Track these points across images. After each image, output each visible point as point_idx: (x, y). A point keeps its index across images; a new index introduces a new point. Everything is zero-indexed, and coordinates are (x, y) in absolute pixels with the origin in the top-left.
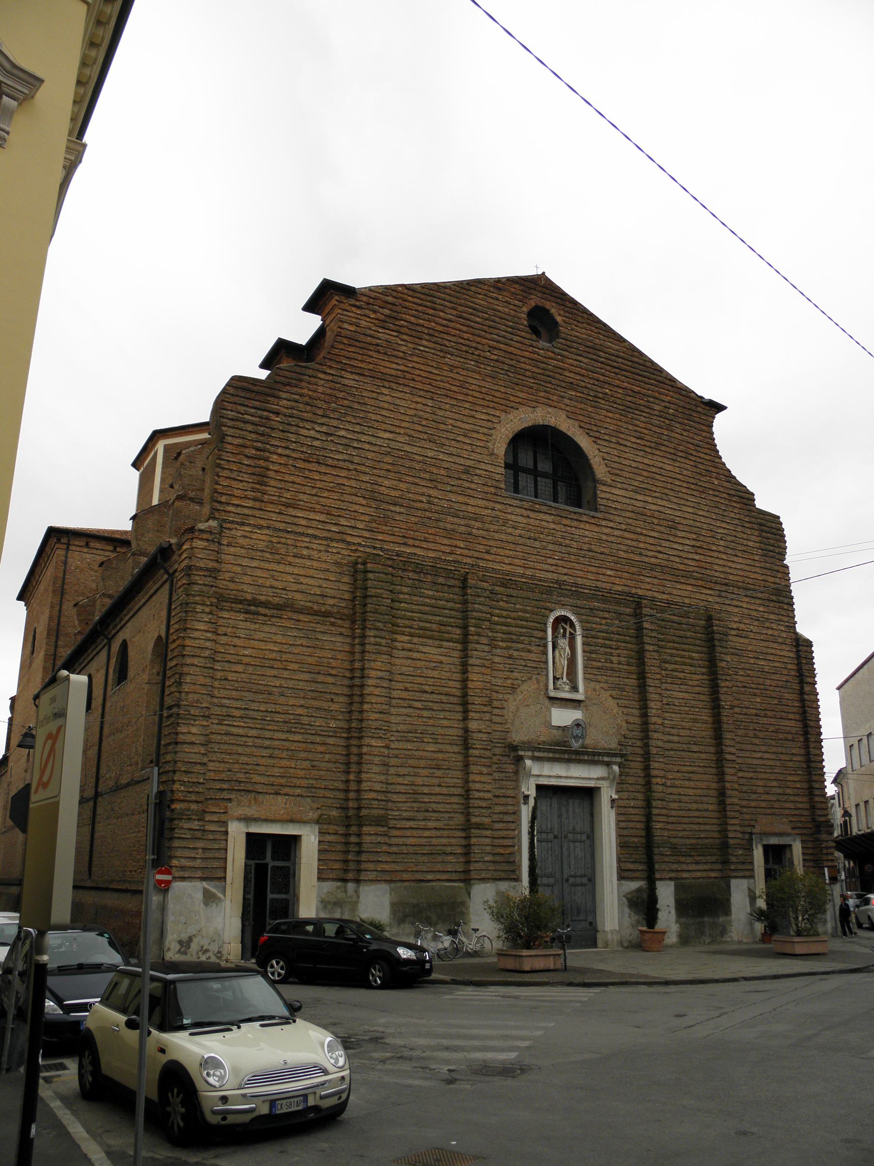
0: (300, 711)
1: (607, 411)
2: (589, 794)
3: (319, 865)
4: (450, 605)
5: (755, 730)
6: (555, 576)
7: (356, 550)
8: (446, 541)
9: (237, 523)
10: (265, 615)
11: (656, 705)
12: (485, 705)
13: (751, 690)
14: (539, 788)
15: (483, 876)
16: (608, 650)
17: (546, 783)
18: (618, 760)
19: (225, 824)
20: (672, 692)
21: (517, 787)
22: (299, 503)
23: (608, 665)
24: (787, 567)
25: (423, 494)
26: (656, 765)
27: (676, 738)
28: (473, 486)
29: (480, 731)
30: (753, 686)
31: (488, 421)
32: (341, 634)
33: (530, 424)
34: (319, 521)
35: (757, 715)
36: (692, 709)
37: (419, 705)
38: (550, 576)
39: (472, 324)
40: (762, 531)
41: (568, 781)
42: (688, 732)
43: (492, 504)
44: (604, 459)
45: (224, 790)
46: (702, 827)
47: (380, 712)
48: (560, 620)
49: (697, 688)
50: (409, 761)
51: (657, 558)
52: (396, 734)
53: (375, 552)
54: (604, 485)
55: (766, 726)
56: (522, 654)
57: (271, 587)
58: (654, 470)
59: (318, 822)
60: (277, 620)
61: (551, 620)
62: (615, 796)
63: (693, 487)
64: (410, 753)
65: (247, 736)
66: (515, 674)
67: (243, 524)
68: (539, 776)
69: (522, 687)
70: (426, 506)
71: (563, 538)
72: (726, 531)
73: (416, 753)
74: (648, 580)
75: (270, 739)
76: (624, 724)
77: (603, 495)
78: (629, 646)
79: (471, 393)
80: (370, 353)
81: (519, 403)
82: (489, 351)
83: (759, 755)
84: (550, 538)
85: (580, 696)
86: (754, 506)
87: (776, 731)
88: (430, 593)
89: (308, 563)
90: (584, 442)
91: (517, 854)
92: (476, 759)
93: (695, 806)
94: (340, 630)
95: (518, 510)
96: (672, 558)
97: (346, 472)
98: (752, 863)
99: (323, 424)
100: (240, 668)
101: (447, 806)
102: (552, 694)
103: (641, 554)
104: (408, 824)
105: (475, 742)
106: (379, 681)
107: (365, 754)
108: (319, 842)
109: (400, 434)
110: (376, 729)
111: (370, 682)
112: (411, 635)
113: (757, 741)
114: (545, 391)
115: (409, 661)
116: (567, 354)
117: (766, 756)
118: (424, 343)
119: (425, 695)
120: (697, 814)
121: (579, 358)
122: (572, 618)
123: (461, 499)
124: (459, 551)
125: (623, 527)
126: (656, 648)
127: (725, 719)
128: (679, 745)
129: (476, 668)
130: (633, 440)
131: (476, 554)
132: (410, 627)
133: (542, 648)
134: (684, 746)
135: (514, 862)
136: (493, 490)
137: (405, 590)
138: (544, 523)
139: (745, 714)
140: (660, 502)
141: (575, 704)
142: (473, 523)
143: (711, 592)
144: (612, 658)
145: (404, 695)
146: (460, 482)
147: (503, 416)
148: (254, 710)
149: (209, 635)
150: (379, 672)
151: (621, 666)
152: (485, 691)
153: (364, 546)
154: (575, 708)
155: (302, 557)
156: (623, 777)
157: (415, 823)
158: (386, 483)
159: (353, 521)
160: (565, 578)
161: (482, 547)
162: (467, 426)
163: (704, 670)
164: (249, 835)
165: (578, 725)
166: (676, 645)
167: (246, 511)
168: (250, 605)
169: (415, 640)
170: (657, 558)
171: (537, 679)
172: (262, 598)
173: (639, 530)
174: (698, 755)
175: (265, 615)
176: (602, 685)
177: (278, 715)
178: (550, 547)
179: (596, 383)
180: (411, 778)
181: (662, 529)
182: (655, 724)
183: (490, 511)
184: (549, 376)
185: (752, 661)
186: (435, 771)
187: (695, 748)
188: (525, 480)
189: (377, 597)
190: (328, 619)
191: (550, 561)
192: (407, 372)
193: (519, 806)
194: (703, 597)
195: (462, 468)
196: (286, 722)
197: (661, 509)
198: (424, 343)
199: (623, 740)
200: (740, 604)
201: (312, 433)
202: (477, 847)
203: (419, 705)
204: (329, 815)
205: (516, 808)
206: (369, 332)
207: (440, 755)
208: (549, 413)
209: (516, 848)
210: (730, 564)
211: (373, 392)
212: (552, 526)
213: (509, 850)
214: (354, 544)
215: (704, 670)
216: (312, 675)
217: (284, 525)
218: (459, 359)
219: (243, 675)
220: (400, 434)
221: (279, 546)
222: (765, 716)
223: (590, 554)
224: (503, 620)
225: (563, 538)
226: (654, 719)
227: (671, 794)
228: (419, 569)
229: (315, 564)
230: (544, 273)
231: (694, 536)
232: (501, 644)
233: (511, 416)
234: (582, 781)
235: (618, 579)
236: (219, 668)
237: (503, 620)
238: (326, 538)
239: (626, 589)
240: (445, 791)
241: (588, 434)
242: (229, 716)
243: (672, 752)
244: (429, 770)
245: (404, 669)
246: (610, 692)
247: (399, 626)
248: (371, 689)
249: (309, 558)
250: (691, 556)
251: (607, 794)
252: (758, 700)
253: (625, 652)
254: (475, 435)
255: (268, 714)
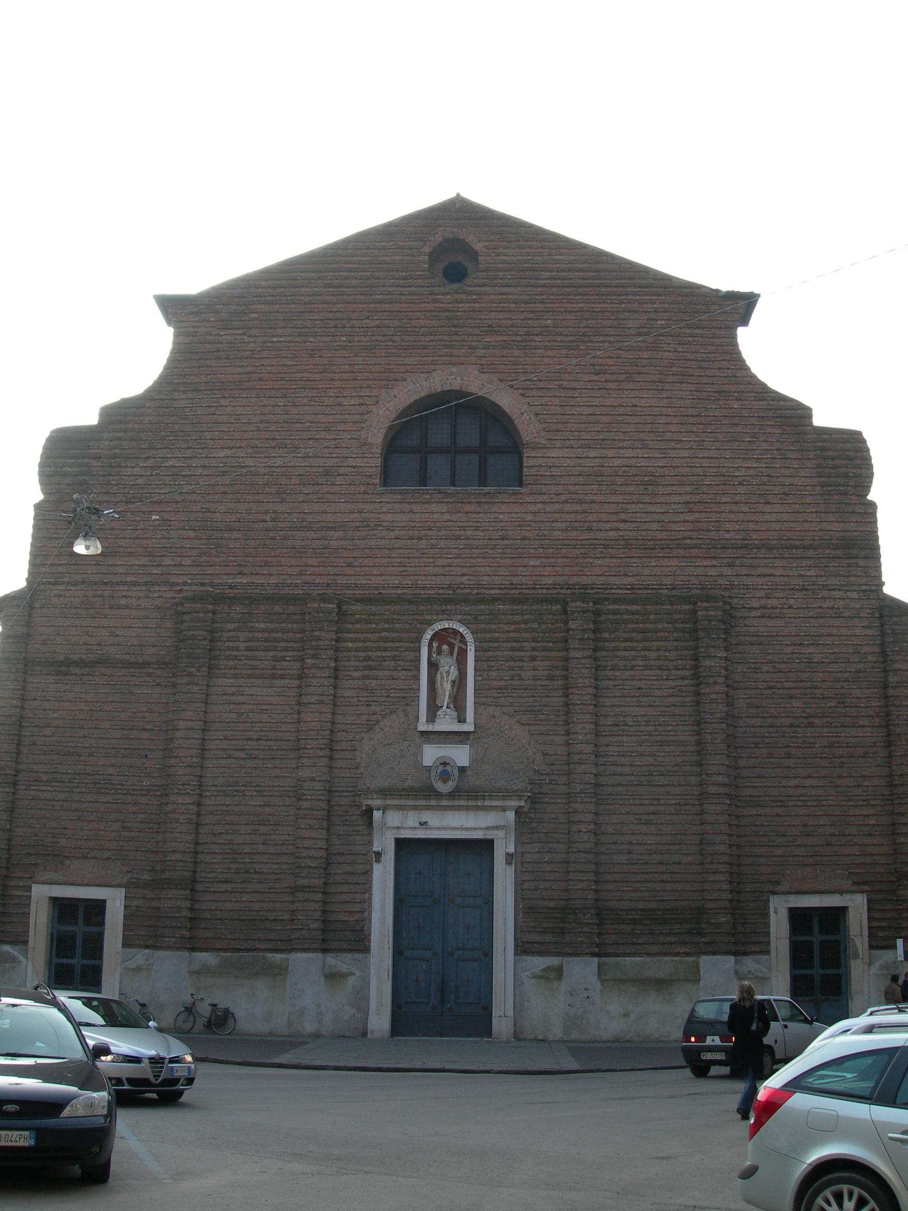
0: (111, 770)
1: (546, 348)
2: (486, 846)
3: (124, 930)
4: (290, 635)
5: (788, 746)
6: (447, 580)
7: (181, 590)
8: (294, 562)
9: (50, 583)
10: (75, 675)
11: (583, 728)
12: (321, 749)
13: (785, 692)
14: (401, 844)
15: (306, 946)
16: (517, 664)
17: (410, 836)
18: (515, 803)
19: (29, 889)
20: (623, 709)
21: (370, 842)
22: (118, 550)
23: (516, 683)
24: (873, 505)
25: (266, 512)
26: (580, 807)
27: (627, 769)
28: (336, 489)
29: (313, 780)
30: (787, 685)
31: (362, 404)
32: (158, 684)
33: (423, 394)
34: (140, 565)
35: (792, 726)
36: (660, 728)
37: (242, 754)
38: (438, 580)
39: (345, 290)
40: (825, 458)
41: (443, 832)
42: (651, 759)
43: (361, 506)
44: (537, 415)
45: (31, 855)
46: (669, 887)
47: (190, 766)
48: (440, 637)
49: (671, 699)
50: (228, 818)
51: (617, 529)
52: (213, 788)
53: (202, 589)
54: (533, 448)
55: (812, 740)
56: (383, 682)
57: (85, 644)
58: (622, 410)
59: (126, 886)
60: (90, 678)
61: (428, 635)
62: (511, 850)
63: (691, 420)
64: (230, 808)
65: (54, 800)
66: (372, 708)
67: (56, 583)
68: (398, 828)
69: (382, 723)
70: (270, 525)
71: (463, 528)
72: (751, 472)
73: (237, 809)
74: (600, 562)
75: (79, 801)
76: (539, 757)
77: (532, 462)
78: (555, 654)
79: (337, 376)
80: (208, 362)
81: (407, 372)
82: (367, 318)
83: (794, 782)
84: (444, 532)
85: (469, 727)
86: (811, 424)
87: (831, 746)
88: (262, 626)
89: (126, 612)
90: (505, 400)
91: (367, 921)
92: (306, 812)
93: (657, 858)
94: (158, 680)
95: (397, 506)
96: (646, 526)
97: (174, 505)
98: (768, 933)
99: (148, 458)
100: (48, 731)
101: (275, 866)
102: (423, 726)
103: (590, 530)
104: (224, 887)
105: (305, 792)
106: (190, 732)
107: (169, 812)
108: (125, 907)
109: (241, 447)
110: (184, 784)
111: (179, 734)
112: (235, 677)
113: (791, 762)
114: (447, 347)
115: (232, 706)
116: (488, 289)
117: (808, 782)
118: (280, 331)
119: (250, 743)
120: (661, 868)
121: (506, 290)
122: (462, 629)
123: (316, 507)
124: (310, 570)
125: (563, 498)
126: (590, 653)
127: (709, 737)
128: (633, 778)
129: (312, 706)
130: (587, 377)
131: (333, 571)
132: (235, 668)
133: (414, 673)
134: (642, 779)
135: (362, 930)
136: (362, 488)
137: (231, 626)
138: (436, 516)
139: (771, 726)
140: (629, 453)
141: (460, 737)
142: (331, 533)
143: (714, 562)
144: (523, 673)
145: (224, 744)
146: (317, 488)
147: (383, 392)
148: (63, 773)
149: (14, 702)
150: (190, 723)
151: (539, 683)
152: (323, 733)
153: (190, 585)
154: (461, 742)
155: (120, 607)
156: (534, 825)
157: (234, 886)
158: (221, 507)
159: (178, 559)
160: (464, 579)
161: (342, 560)
162: (330, 419)
163: (686, 673)
164: (54, 900)
165: (445, 764)
166: (635, 644)
167: (60, 569)
168: (60, 666)
169: (241, 681)
170: (617, 529)
171: (404, 711)
172: (76, 657)
173: (590, 497)
174: (668, 789)
175: (75, 675)
176: (505, 709)
177: (88, 777)
178: (442, 544)
179: (531, 316)
180: (230, 837)
181: (632, 489)
182: (581, 753)
183: (357, 515)
184: (455, 326)
185: (789, 650)
186: (260, 827)
187: (663, 780)
188: (438, 464)
189: (193, 640)
190: (145, 670)
191: (441, 562)
192: (254, 373)
193: (372, 865)
194: (699, 571)
195: (321, 470)
196: (96, 783)
197: (633, 462)
198: (280, 331)
199: (536, 777)
200: (772, 571)
201: (137, 471)
202: (302, 913)
203: (242, 754)
204: (138, 879)
205: (369, 868)
206: (208, 338)
207: (267, 810)
208: (452, 374)
209: (366, 914)
210: (754, 518)
211: (210, 407)
212: (448, 517)
213: (357, 917)
214: (178, 584)
215: (686, 673)
216: (125, 732)
217: (101, 576)
218: (325, 339)
219: (52, 738)
220: (241, 447)
221: (95, 599)
222: (811, 725)
223: (506, 542)
224: (360, 644)
225: (463, 528)
226: (579, 748)
227: (615, 843)
228: (252, 600)
229: (134, 612)
230: (458, 195)
231: (688, 489)
232: (355, 674)
233: (395, 392)
234: (464, 832)
235: (548, 569)
236: (28, 734)
237: (360, 644)
238: (146, 584)
239: (561, 580)
240: (272, 850)
241: (511, 387)
242: (37, 781)
243: (620, 789)
244: (252, 827)
245: (225, 715)
246: (518, 717)
247: (221, 669)
248: (180, 741)
249: (127, 607)
250: (681, 517)
251: (504, 846)
252: (797, 703)
253: (547, 663)
254: (341, 427)
255: (77, 777)
